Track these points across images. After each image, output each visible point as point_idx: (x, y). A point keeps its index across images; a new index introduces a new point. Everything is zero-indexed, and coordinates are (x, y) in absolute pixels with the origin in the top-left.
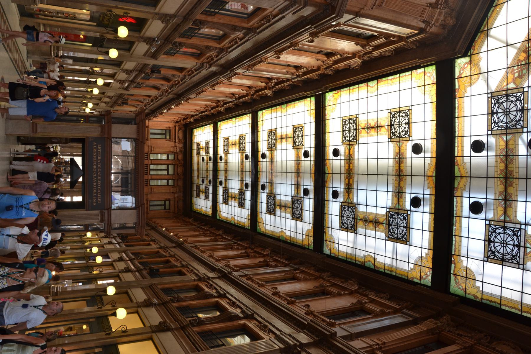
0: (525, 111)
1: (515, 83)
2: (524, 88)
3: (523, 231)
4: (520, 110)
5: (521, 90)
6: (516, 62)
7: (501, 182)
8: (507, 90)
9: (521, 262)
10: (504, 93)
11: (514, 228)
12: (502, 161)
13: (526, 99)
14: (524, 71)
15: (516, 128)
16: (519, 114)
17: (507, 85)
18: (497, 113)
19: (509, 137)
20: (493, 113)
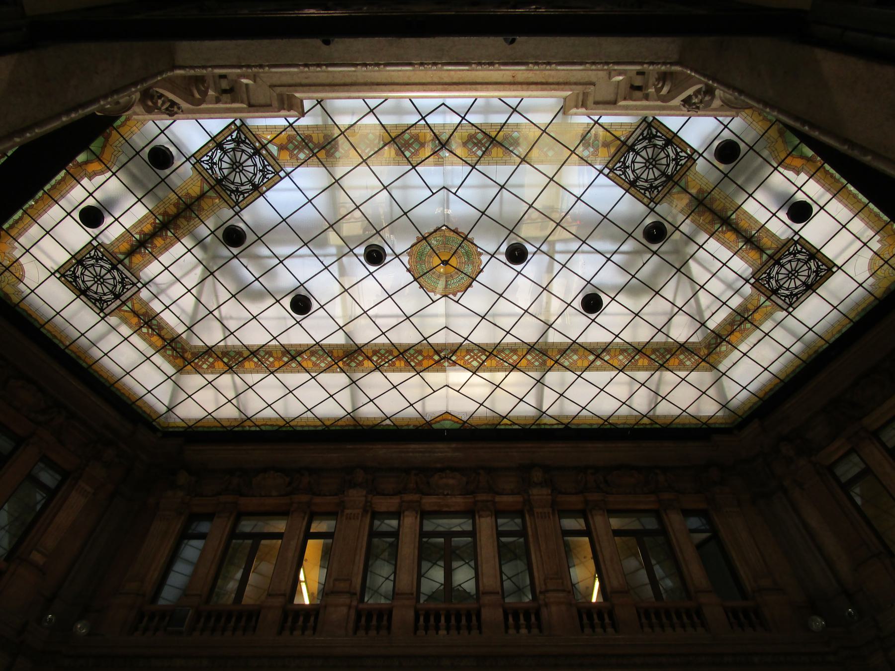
0: (256, 192)
1: (279, 154)
2: (282, 169)
3: (135, 289)
4: (253, 185)
5: (278, 169)
6: (307, 133)
7: (155, 223)
8: (264, 146)
9: (107, 311)
10: (257, 144)
11: (127, 278)
12: (176, 205)
13: (271, 183)
14: (302, 156)
15: (230, 196)
16: (249, 187)
17: (270, 142)
18: (225, 152)
19: (212, 193)
20: (220, 146)
